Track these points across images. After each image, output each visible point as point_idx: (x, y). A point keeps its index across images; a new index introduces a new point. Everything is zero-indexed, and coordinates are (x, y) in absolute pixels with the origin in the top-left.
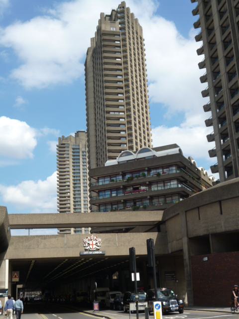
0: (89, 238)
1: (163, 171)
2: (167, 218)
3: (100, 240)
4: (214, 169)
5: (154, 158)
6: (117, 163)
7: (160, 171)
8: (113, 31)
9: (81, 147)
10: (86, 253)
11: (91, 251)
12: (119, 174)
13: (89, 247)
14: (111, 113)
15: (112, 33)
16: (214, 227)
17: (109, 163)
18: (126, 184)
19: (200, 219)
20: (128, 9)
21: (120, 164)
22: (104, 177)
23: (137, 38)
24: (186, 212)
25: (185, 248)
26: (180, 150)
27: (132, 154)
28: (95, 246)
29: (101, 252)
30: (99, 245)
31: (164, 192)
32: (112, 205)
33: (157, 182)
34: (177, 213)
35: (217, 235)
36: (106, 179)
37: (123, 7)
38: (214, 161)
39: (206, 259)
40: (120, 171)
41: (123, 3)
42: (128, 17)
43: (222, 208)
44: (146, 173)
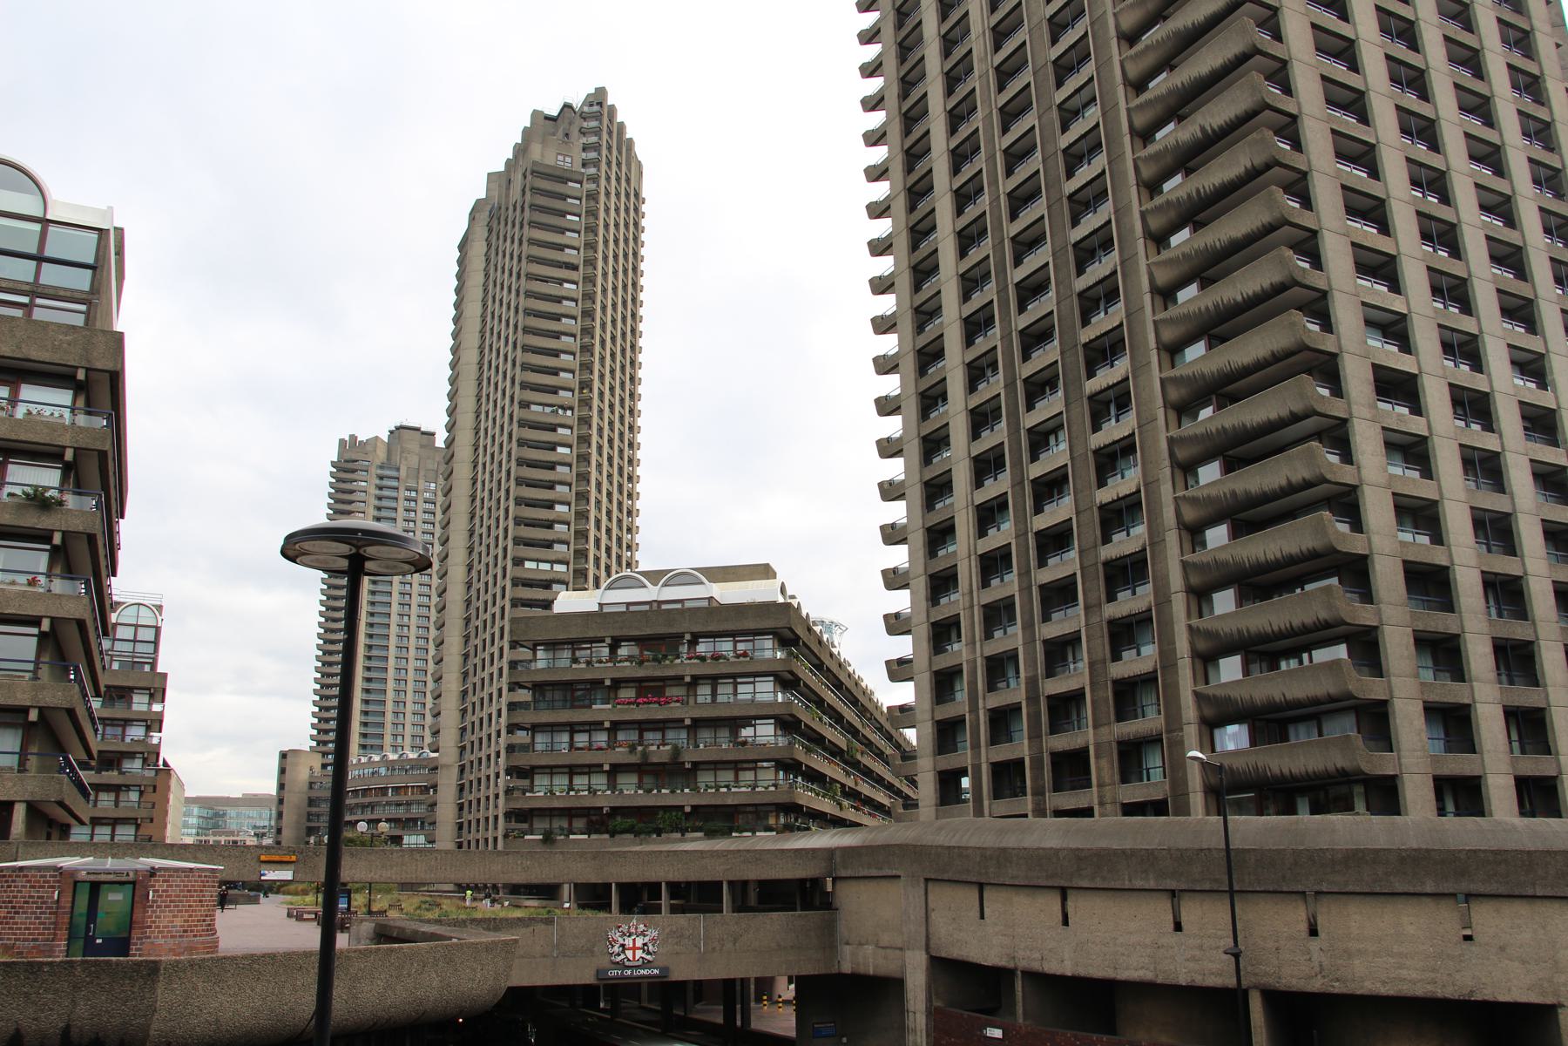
0: (625, 928)
3: (655, 934)
4: (898, 670)
5: (714, 609)
9: (403, 473)
14: (534, 408)
15: (557, 173)
16: (1037, 955)
19: (982, 917)
20: (612, 109)
23: (627, 195)
24: (927, 880)
28: (639, 953)
29: (656, 972)
31: (736, 713)
32: (572, 733)
34: (894, 872)
35: (1041, 981)
37: (600, 104)
39: (997, 1033)
40: (608, 633)
41: (601, 92)
42: (610, 133)
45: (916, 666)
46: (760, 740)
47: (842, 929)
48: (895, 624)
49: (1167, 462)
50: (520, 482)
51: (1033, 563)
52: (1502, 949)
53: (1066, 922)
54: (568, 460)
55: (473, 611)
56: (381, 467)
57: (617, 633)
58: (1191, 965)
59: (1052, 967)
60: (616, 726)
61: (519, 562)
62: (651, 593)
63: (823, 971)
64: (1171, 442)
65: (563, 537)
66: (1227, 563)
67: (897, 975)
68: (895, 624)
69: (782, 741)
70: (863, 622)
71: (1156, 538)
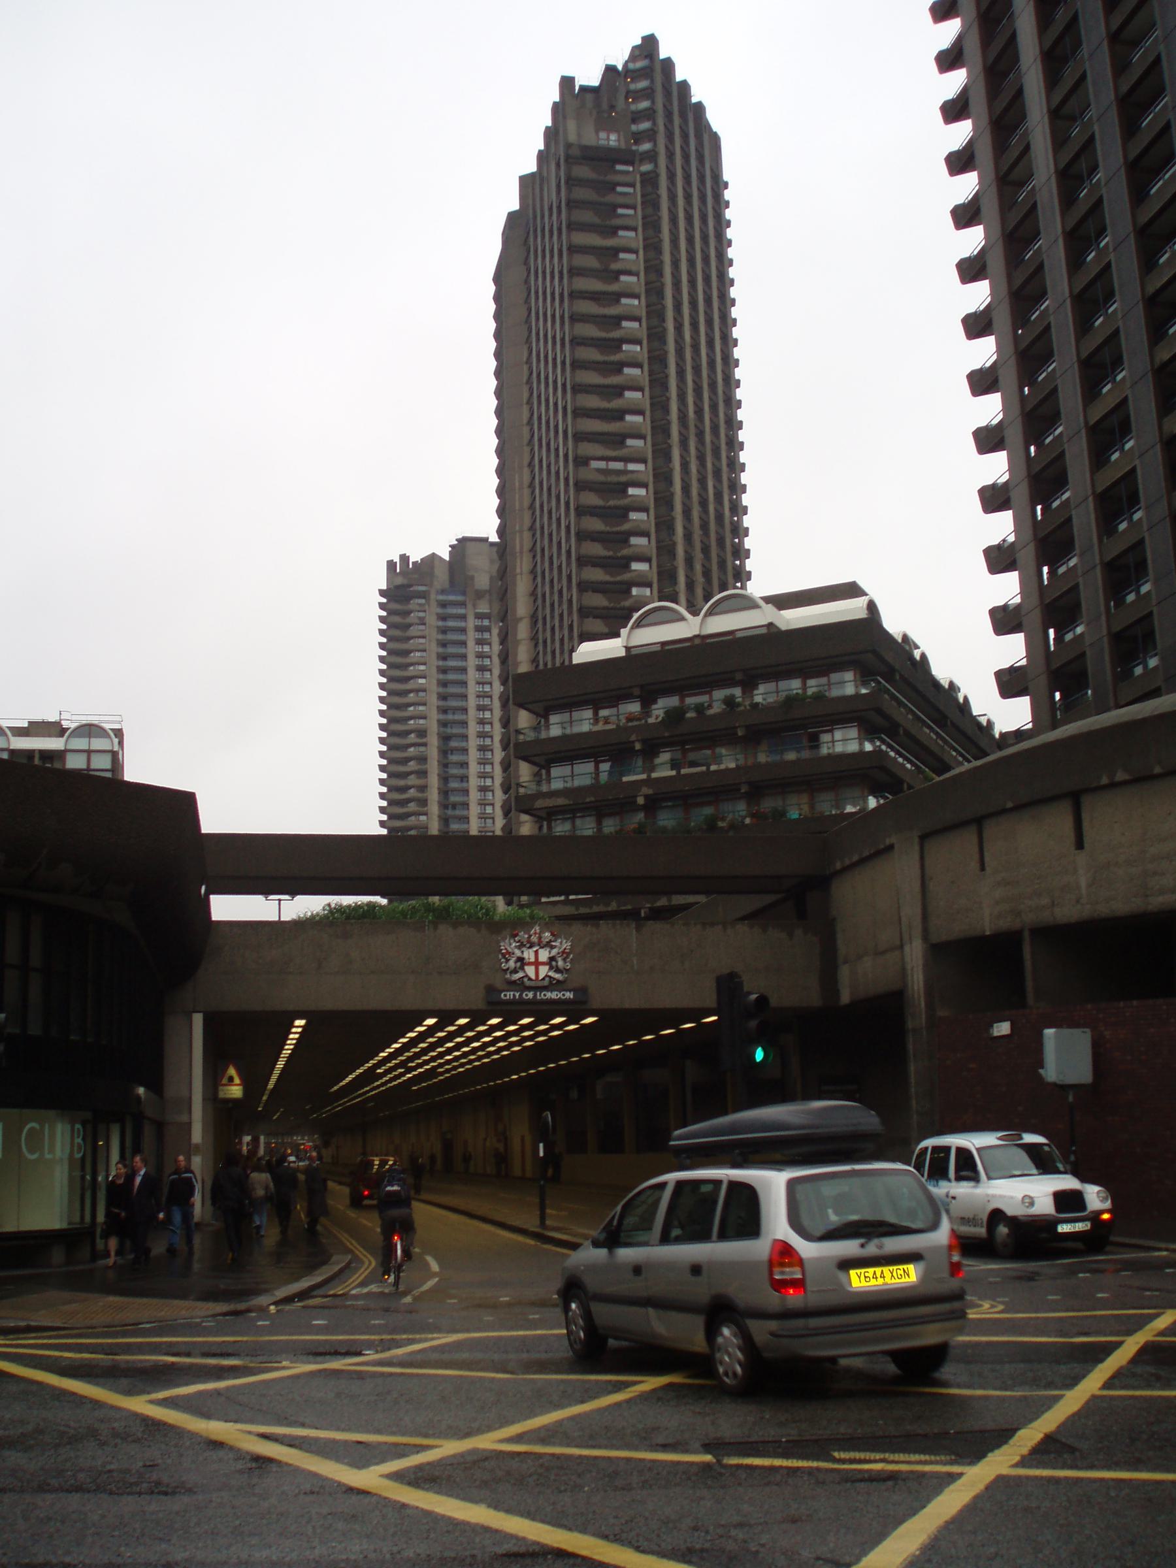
3: (567, 945)
4: (1010, 683)
5: (772, 636)
6: (622, 653)
7: (795, 685)
8: (610, 150)
10: (509, 995)
11: (529, 989)
13: (521, 974)
19: (983, 868)
20: (668, 65)
21: (633, 659)
24: (923, 838)
25: (917, 981)
26: (872, 607)
27: (683, 619)
28: (543, 971)
29: (569, 995)
30: (560, 963)
34: (888, 842)
35: (1054, 936)
36: (576, 715)
38: (1013, 650)
39: (1003, 1028)
43: (1086, 824)
48: (1005, 620)
53: (1080, 844)
56: (443, 592)
59: (1067, 912)
70: (961, 626)
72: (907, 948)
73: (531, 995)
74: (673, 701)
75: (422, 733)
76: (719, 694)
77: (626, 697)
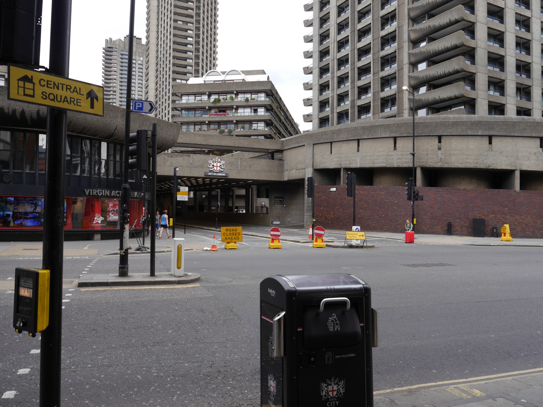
1: (251, 97)
2: (286, 148)
5: (244, 82)
6: (203, 82)
7: (248, 96)
10: (210, 174)
12: (205, 94)
16: (348, 162)
17: (193, 81)
18: (213, 105)
21: (205, 85)
22: (188, 94)
28: (218, 168)
29: (224, 175)
33: (244, 107)
34: (303, 144)
39: (334, 189)
40: (207, 90)
44: (234, 96)
45: (314, 117)
46: (259, 128)
47: (286, 167)
49: (407, 18)
50: (174, 50)
51: (356, 59)
52: (501, 153)
53: (358, 151)
54: (192, 43)
55: (158, 99)
57: (210, 90)
58: (399, 161)
59: (353, 165)
60: (210, 123)
61: (174, 80)
62: (222, 78)
63: (278, 180)
64: (409, 10)
65: (191, 71)
66: (424, 52)
67: (302, 178)
68: (307, 102)
69: (268, 114)
71: (400, 69)
72: (307, 169)
73: (215, 174)
74: (216, 97)
75: (115, 92)
76: (228, 96)
77: (204, 94)
